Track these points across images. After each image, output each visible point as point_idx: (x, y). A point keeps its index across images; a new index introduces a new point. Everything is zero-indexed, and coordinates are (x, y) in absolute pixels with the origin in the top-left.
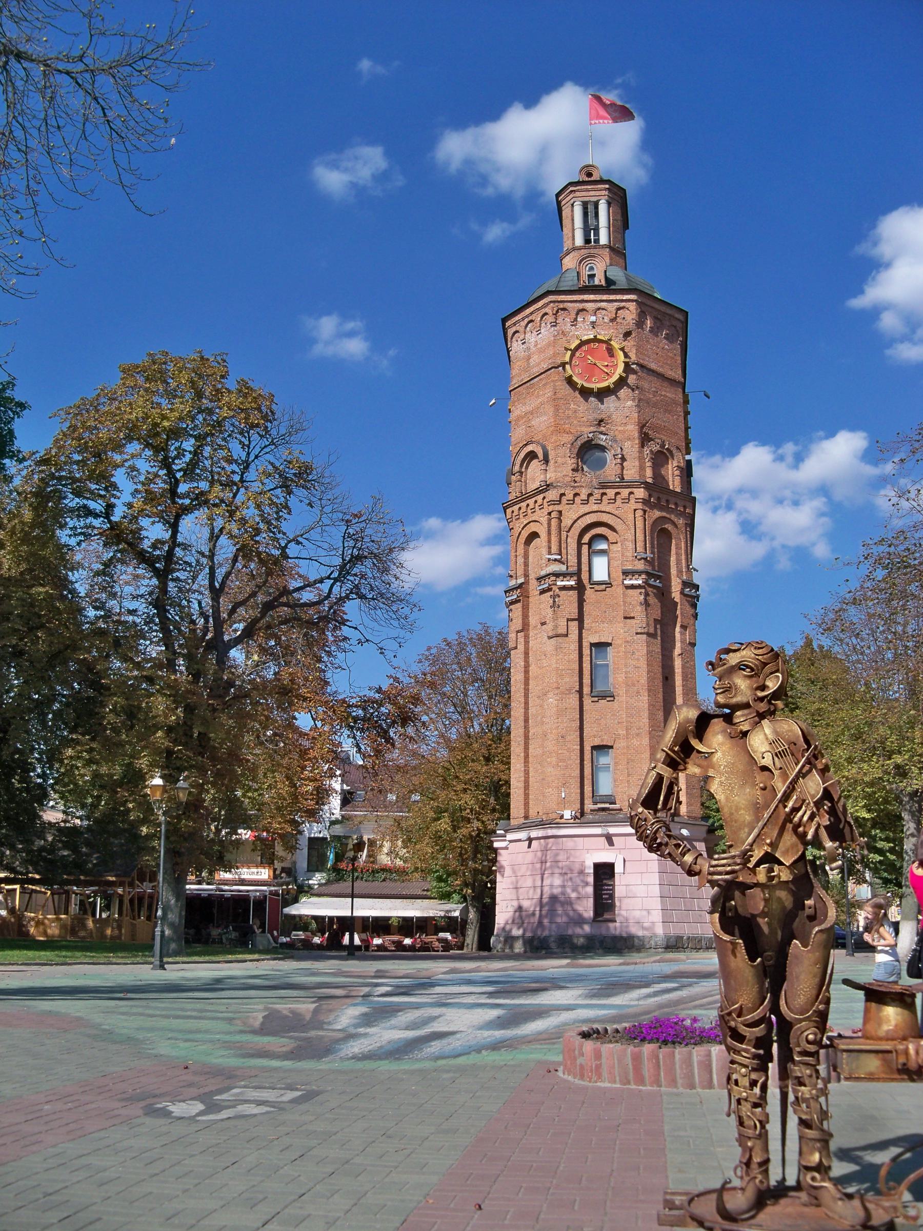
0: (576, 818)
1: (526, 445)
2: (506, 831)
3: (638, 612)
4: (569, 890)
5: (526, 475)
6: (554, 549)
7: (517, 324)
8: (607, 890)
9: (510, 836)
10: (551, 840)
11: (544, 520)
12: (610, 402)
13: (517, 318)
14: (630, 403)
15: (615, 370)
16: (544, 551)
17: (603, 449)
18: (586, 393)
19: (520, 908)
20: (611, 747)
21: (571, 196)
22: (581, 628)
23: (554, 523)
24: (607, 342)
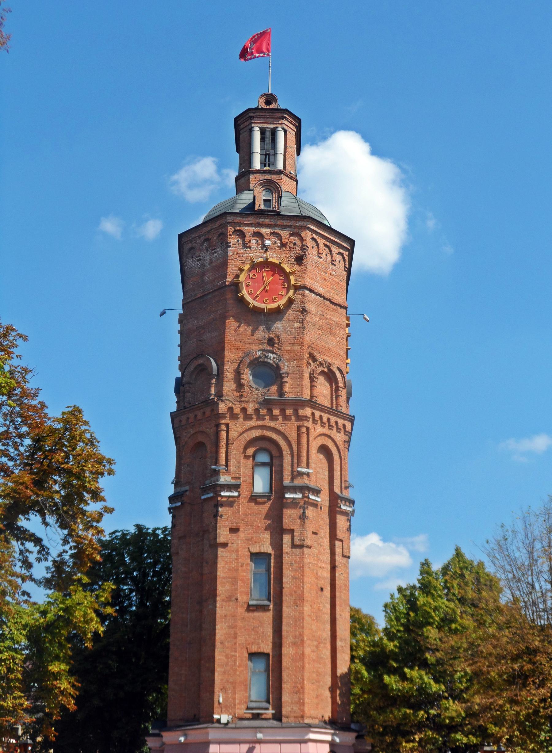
1: (195, 358)
11: (211, 431)
14: (297, 325)
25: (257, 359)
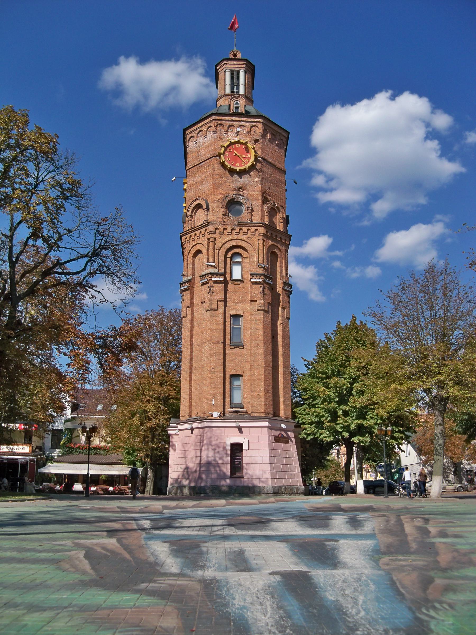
0: (220, 416)
1: (195, 200)
2: (177, 424)
3: (259, 298)
4: (217, 459)
5: (195, 217)
6: (211, 259)
8: (238, 459)
9: (180, 427)
10: (206, 429)
11: (205, 243)
12: (246, 178)
14: (257, 179)
15: (249, 160)
16: (205, 261)
17: (240, 204)
18: (232, 172)
19: (187, 468)
20: (242, 376)
21: (225, 66)
22: (225, 306)
23: (211, 244)
24: (245, 144)
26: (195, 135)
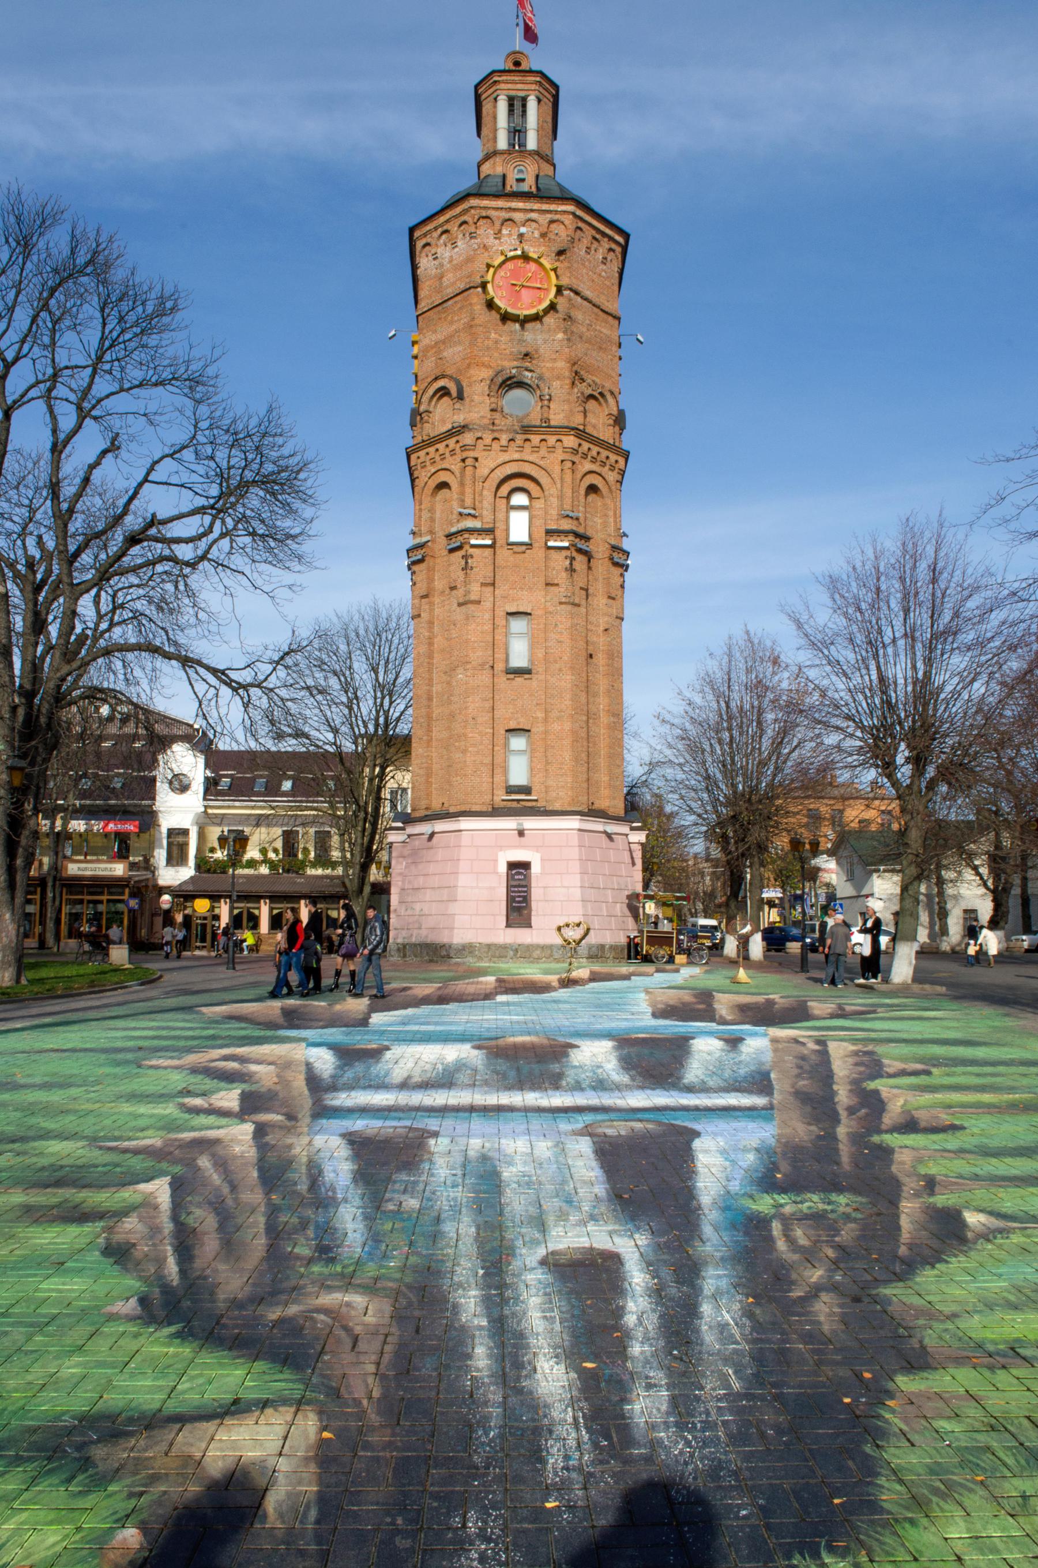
1: (436, 379)
6: (468, 502)
7: (429, 234)
11: (456, 467)
13: (428, 228)
14: (560, 336)
25: (510, 378)
26: (433, 242)
